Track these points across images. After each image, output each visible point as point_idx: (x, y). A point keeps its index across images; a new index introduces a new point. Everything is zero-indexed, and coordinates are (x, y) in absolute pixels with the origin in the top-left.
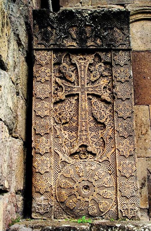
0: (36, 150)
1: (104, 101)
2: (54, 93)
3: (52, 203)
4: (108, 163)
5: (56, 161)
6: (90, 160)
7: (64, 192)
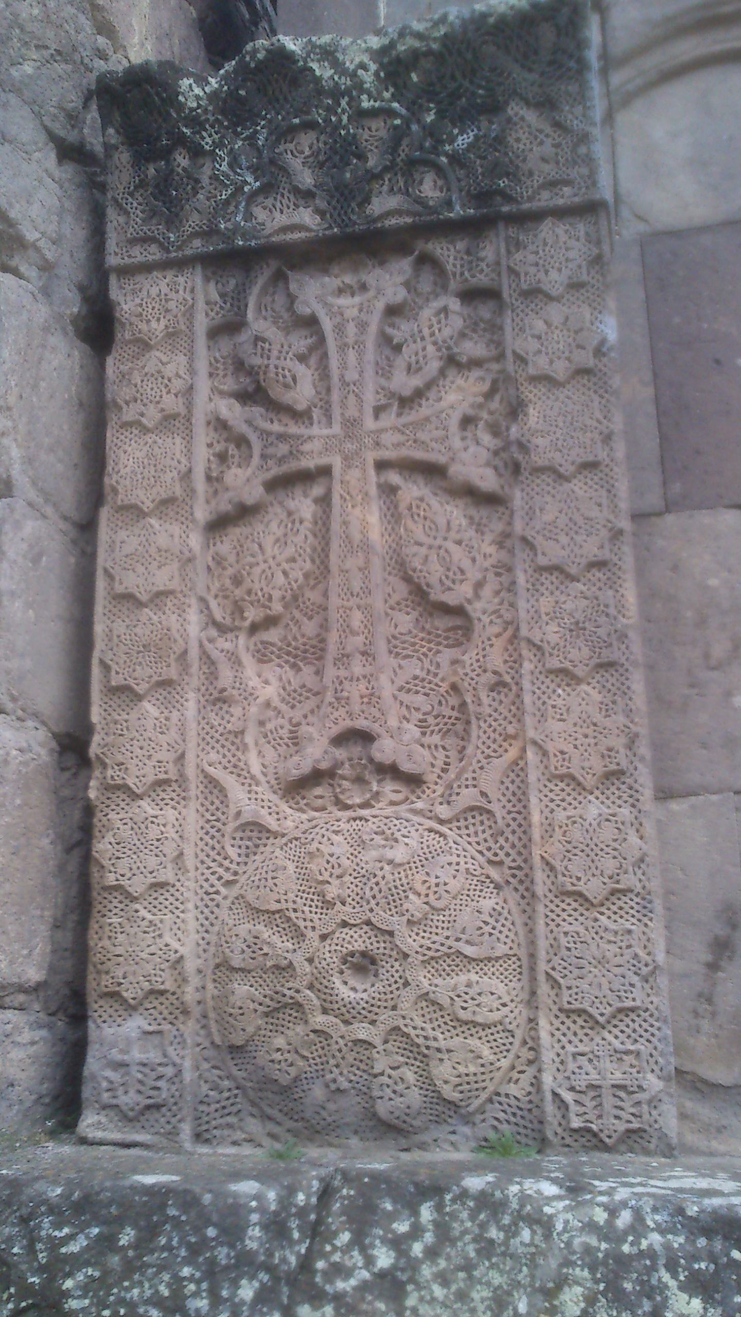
0: (110, 772)
2: (209, 478)
3: (182, 1053)
5: (212, 827)
6: (389, 811)
7: (241, 989)
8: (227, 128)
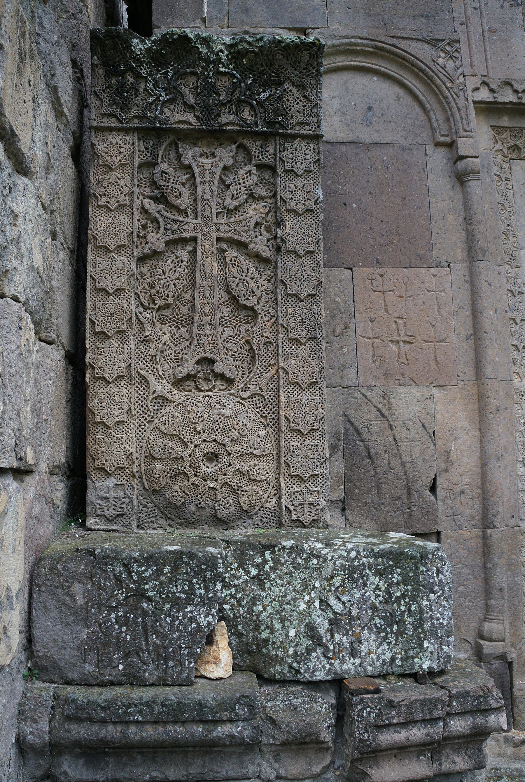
0: (96, 371)
1: (258, 257)
4: (261, 400)
6: (221, 393)
7: (159, 467)
8: (154, 67)
